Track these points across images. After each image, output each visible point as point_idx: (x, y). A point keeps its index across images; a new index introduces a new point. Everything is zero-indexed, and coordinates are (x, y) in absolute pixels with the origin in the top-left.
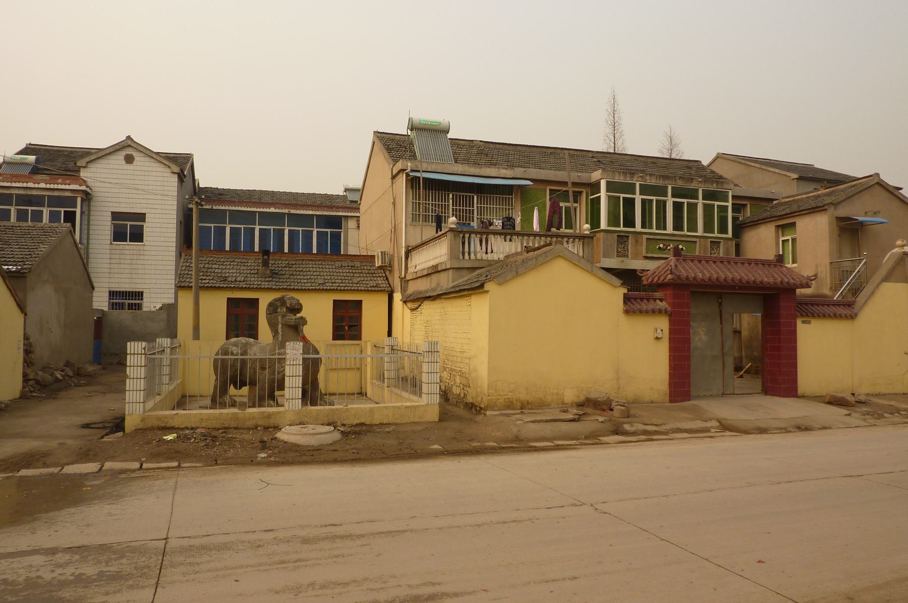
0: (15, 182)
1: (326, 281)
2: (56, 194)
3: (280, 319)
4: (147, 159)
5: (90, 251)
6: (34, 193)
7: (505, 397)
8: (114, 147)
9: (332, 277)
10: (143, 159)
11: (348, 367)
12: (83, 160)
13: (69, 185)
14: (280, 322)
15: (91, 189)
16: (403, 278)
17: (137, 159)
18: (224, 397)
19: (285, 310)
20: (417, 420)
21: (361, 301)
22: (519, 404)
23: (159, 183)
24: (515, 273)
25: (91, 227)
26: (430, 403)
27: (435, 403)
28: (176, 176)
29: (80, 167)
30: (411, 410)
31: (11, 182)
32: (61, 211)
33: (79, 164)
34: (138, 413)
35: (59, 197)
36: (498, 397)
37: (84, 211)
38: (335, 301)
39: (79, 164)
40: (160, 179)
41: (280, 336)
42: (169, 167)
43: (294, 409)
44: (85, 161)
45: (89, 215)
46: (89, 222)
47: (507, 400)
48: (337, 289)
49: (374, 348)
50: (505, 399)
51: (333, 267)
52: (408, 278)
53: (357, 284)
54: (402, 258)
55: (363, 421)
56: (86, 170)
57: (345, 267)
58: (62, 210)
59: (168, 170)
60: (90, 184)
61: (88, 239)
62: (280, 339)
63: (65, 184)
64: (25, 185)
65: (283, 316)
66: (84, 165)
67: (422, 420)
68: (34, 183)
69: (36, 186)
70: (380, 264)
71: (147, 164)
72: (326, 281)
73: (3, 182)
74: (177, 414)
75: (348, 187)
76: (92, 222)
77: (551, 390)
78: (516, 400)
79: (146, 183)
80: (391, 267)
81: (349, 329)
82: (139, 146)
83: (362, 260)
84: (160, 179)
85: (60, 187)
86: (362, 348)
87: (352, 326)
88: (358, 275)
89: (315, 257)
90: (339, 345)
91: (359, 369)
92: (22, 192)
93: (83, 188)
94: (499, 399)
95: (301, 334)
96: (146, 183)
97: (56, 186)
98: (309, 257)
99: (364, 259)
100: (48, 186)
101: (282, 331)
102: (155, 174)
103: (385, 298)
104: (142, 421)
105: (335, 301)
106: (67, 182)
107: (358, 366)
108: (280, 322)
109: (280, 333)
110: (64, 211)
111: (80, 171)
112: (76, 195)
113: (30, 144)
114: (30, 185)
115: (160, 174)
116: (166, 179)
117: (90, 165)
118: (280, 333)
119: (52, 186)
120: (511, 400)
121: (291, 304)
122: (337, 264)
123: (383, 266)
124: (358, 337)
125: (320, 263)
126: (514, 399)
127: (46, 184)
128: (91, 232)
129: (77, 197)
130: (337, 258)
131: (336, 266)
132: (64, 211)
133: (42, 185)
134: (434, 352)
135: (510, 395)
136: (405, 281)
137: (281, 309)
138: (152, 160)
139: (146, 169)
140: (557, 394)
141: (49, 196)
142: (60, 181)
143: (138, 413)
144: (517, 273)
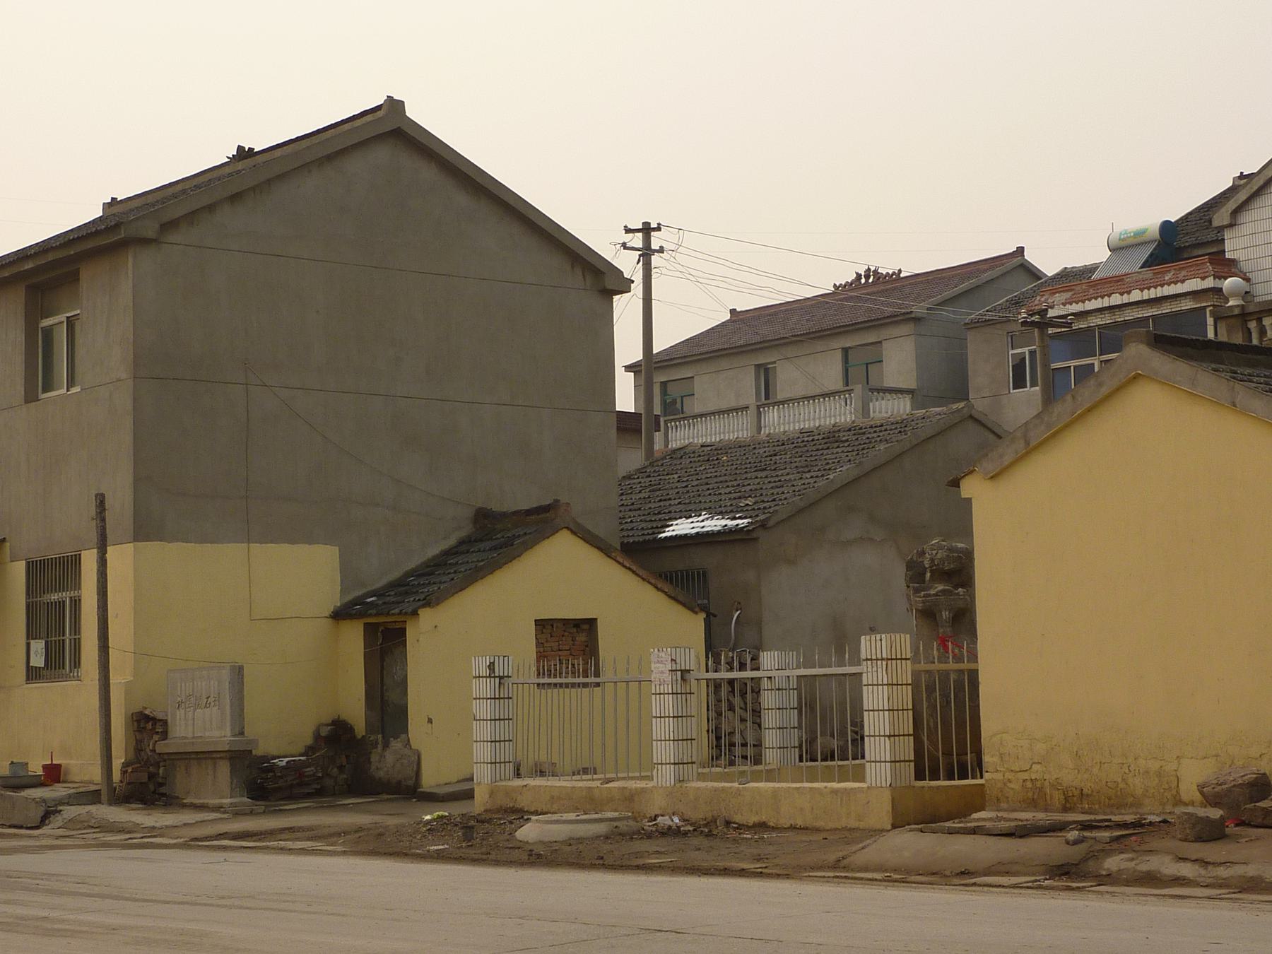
2: (1166, 309)
6: (1129, 315)
7: (1025, 776)
12: (1223, 210)
20: (853, 823)
22: (1058, 798)
24: (1022, 442)
26: (874, 785)
27: (884, 785)
29: (1221, 229)
30: (842, 800)
33: (1216, 223)
34: (486, 782)
36: (1009, 776)
39: (1216, 223)
43: (664, 785)
47: (1029, 784)
50: (1024, 781)
55: (764, 819)
56: (1237, 231)
64: (1106, 302)
66: (1226, 222)
67: (862, 825)
69: (1126, 299)
74: (526, 786)
77: (1142, 762)
78: (1052, 785)
94: (1010, 781)
104: (490, 797)
111: (1224, 240)
112: (1203, 305)
114: (1116, 299)
117: (1245, 217)
120: (1038, 784)
126: (1047, 783)
127: (1142, 290)
133: (1136, 295)
134: (877, 660)
135: (1037, 772)
140: (1159, 774)
143: (486, 782)
144: (1027, 443)
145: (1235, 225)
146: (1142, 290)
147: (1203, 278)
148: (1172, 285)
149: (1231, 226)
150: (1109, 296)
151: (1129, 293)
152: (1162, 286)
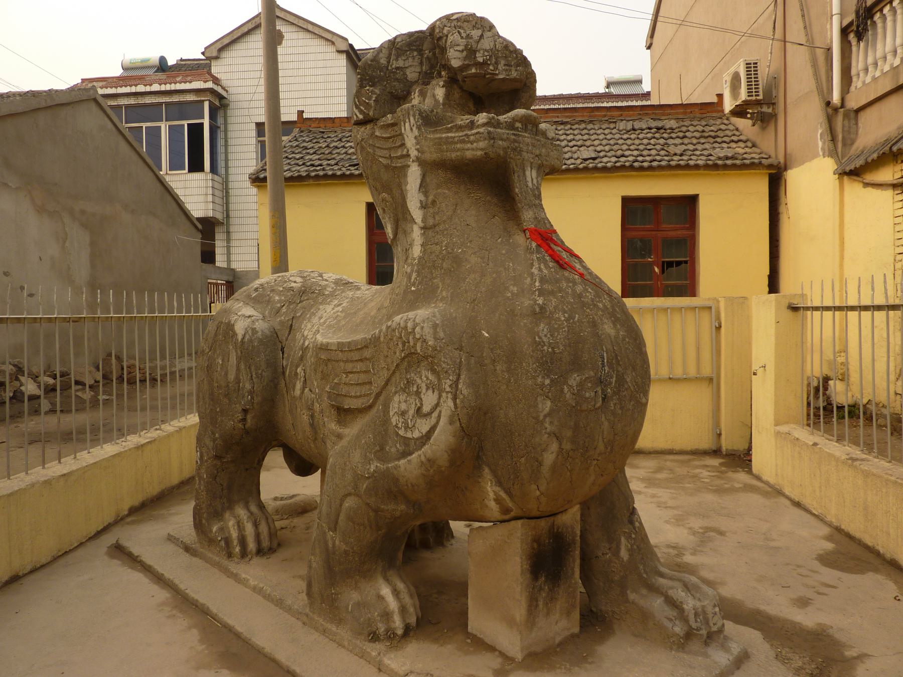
0: (121, 87)
1: (602, 154)
2: (175, 99)
3: (410, 134)
4: (302, 35)
5: (231, 185)
6: (148, 100)
8: (254, 21)
9: (616, 147)
10: (295, 35)
11: (678, 372)
13: (190, 82)
14: (414, 153)
15: (227, 91)
16: (836, 110)
17: (286, 36)
18: (227, 515)
19: (440, 93)
21: (692, 201)
23: (319, 72)
25: (230, 149)
28: (344, 56)
31: (116, 87)
32: (184, 125)
35: (180, 103)
37: (219, 125)
38: (627, 202)
40: (320, 64)
41: (416, 234)
42: (333, 43)
44: (215, 48)
45: (226, 131)
46: (226, 141)
48: (631, 167)
49: (790, 313)
51: (614, 131)
52: (853, 103)
53: (681, 155)
54: (829, 50)
56: (219, 62)
57: (643, 130)
58: (185, 123)
59: (331, 49)
60: (224, 83)
61: (227, 167)
62: (417, 251)
63: (185, 82)
64: (133, 89)
65: (428, 121)
68: (145, 85)
69: (148, 89)
70: (743, 95)
71: (301, 43)
72: (602, 154)
73: (106, 88)
75: (610, 80)
76: (230, 142)
79: (301, 72)
80: (774, 104)
81: (663, 272)
82: (288, 15)
83: (681, 116)
84: (320, 64)
85: (179, 87)
86: (718, 318)
87: (670, 264)
88: (678, 141)
89: (567, 117)
90: (652, 310)
91: (711, 380)
92: (132, 101)
93: (210, 85)
95: (527, 216)
96: (301, 72)
97: (173, 87)
98: (555, 117)
99: (685, 113)
100: (163, 88)
101: (423, 206)
102: (312, 57)
103: (762, 186)
105: (627, 202)
106: (189, 78)
107: (707, 371)
108: (414, 153)
109: (417, 214)
110: (188, 124)
112: (202, 99)
113: (182, 60)
114: (141, 88)
115: (320, 57)
116: (329, 63)
117: (224, 54)
118: (417, 214)
119: (168, 87)
121: (471, 52)
122: (622, 125)
123: (750, 101)
124: (689, 288)
125: (583, 126)
127: (160, 84)
128: (230, 156)
129: (203, 101)
130: (621, 115)
131: (621, 128)
132: (188, 124)
133: (156, 87)
136: (846, 116)
137: (423, 94)
138: (308, 35)
139: (301, 50)
141: (167, 104)
142: (178, 79)
145: (219, 58)
146: (160, 84)
147: (205, 82)
148: (183, 84)
149: (217, 58)
150: (136, 85)
151: (151, 85)
152: (175, 83)
